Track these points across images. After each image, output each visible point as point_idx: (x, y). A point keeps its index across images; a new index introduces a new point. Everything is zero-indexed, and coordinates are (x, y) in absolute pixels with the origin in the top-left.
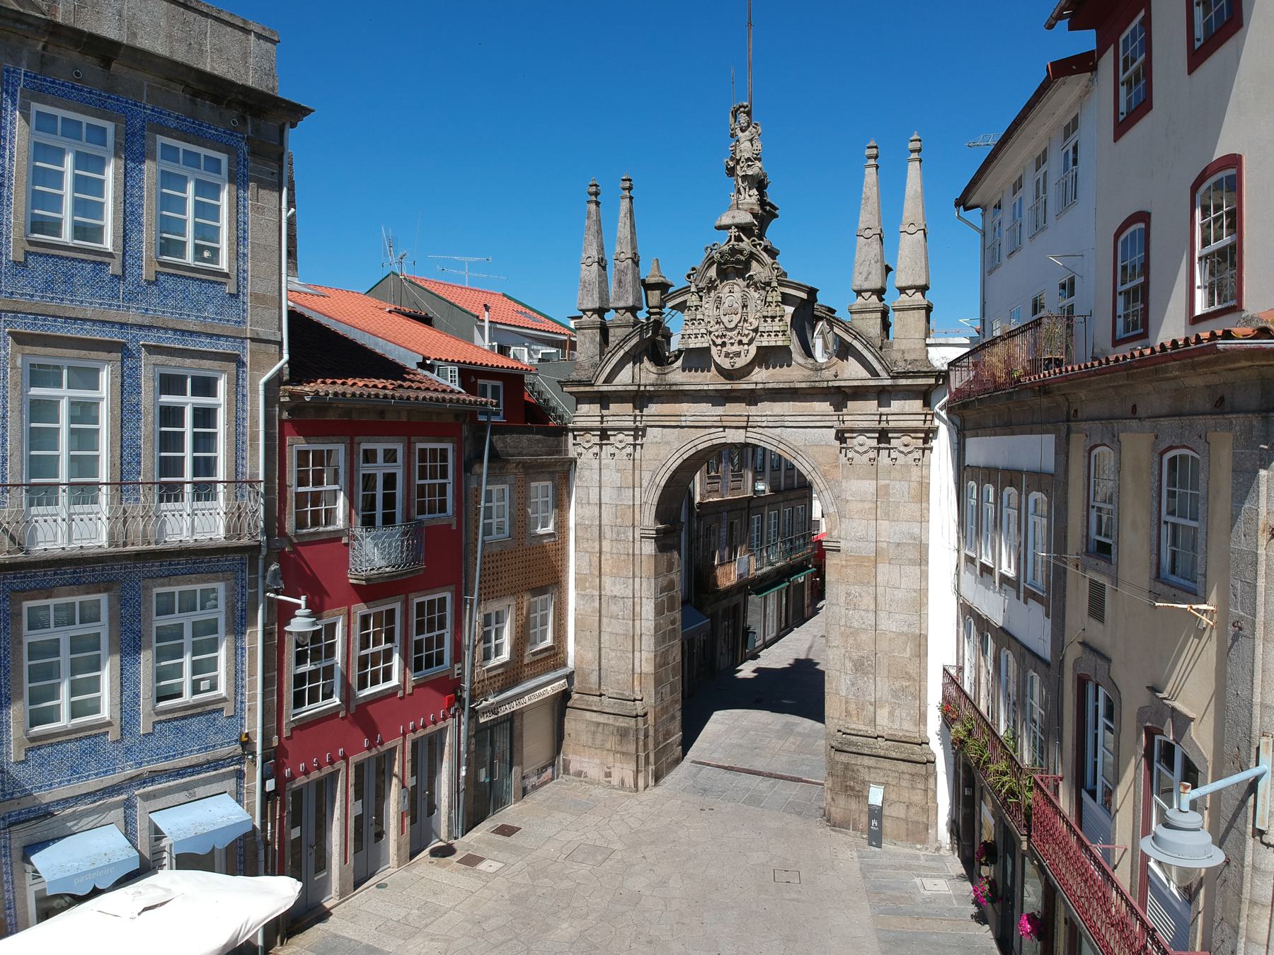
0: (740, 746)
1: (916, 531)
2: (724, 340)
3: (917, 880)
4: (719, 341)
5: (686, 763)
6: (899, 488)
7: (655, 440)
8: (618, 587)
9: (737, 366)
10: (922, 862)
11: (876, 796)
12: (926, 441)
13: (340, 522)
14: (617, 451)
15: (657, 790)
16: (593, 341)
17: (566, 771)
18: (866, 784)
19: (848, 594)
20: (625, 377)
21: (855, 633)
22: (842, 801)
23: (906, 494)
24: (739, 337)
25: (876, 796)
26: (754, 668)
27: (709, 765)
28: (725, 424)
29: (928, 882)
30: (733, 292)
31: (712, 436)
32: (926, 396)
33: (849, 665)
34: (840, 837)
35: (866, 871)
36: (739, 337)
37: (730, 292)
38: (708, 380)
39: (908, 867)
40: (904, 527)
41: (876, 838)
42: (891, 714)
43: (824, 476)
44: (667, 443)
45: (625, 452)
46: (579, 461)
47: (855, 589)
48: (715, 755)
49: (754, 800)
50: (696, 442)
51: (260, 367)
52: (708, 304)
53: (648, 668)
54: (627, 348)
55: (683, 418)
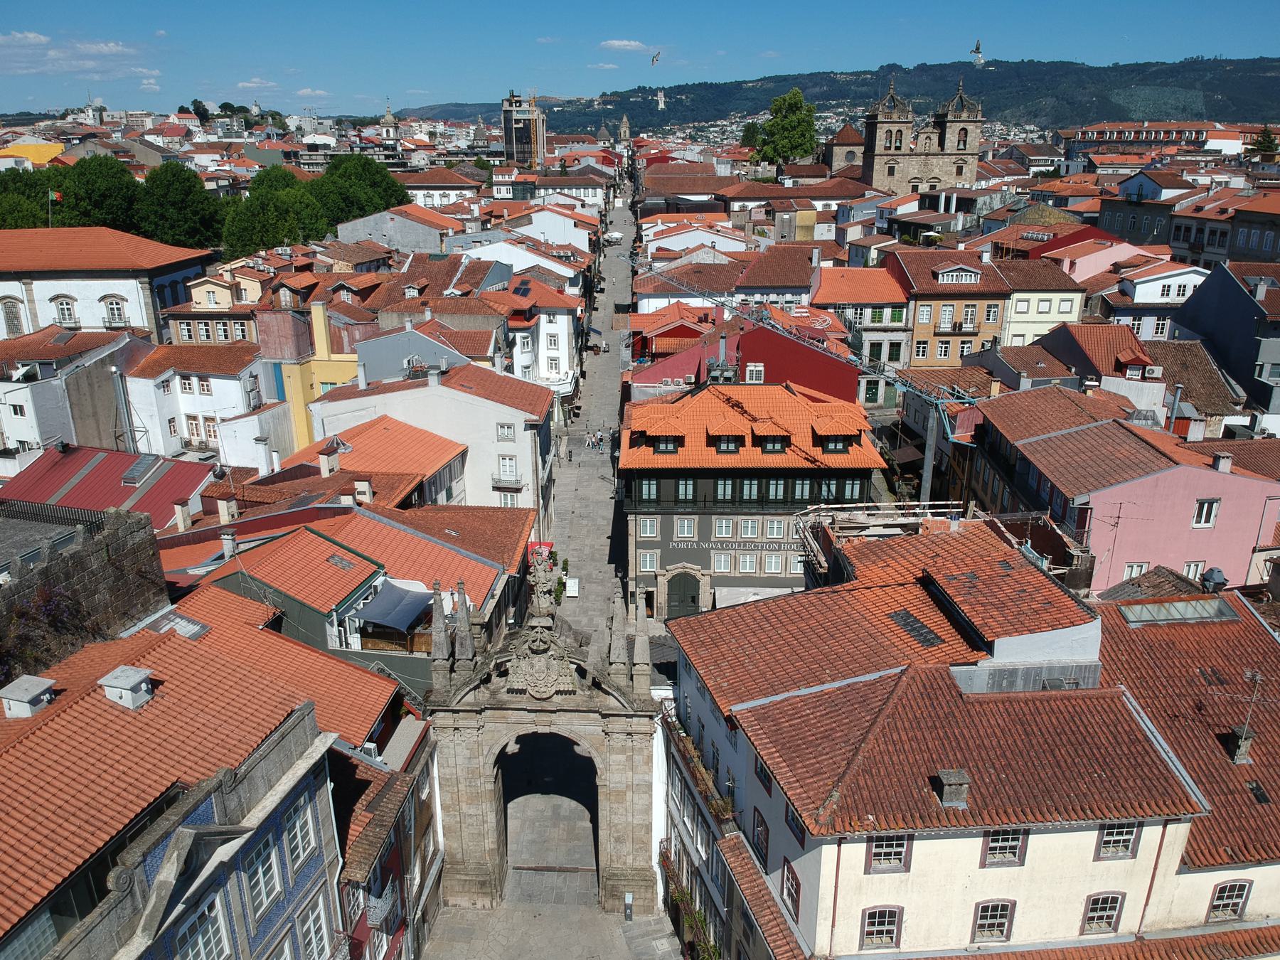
0: (533, 842)
3: (654, 943)
5: (510, 871)
6: (638, 758)
10: (654, 927)
11: (629, 899)
13: (362, 906)
15: (504, 905)
16: (444, 677)
17: (446, 904)
18: (623, 893)
19: (611, 808)
20: (470, 698)
21: (616, 825)
22: (611, 901)
25: (629, 899)
26: (514, 739)
27: (523, 869)
29: (658, 943)
30: (540, 661)
32: (651, 717)
33: (612, 840)
34: (613, 918)
35: (630, 941)
38: (523, 701)
39: (647, 934)
40: (641, 776)
41: (628, 917)
42: (634, 859)
46: (439, 744)
47: (615, 806)
48: (524, 856)
49: (559, 899)
51: (332, 876)
52: (523, 664)
53: (494, 846)
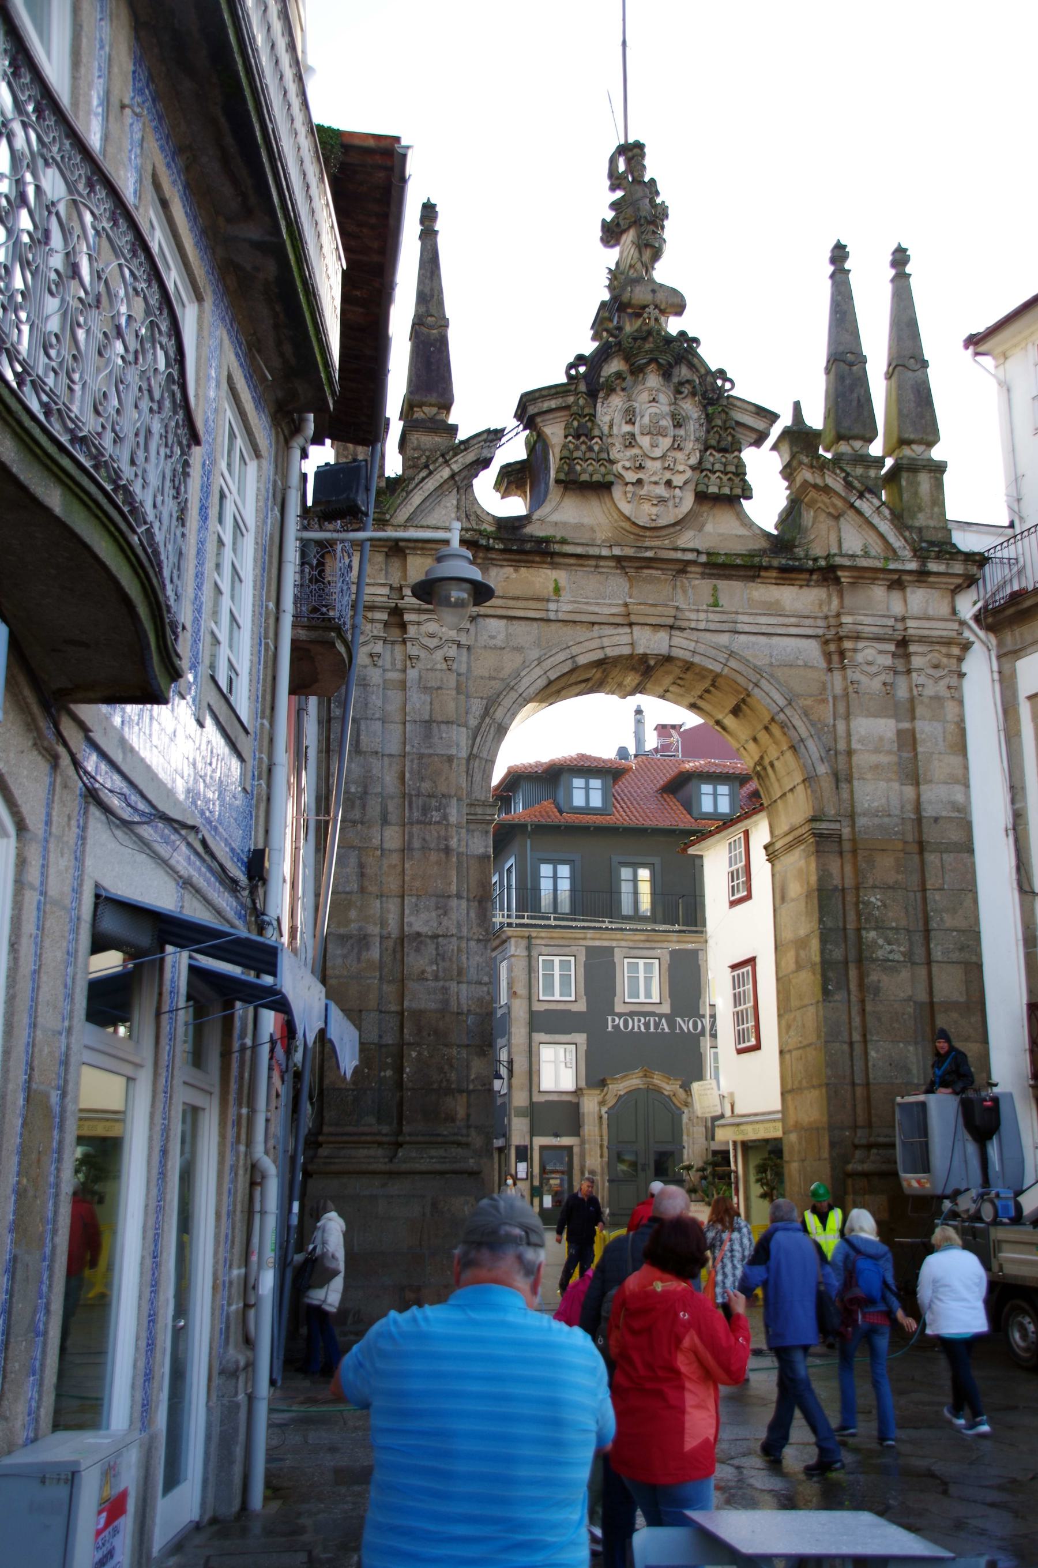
1: (959, 798)
2: (640, 475)
4: (631, 476)
7: (492, 643)
8: (424, 916)
9: (662, 522)
12: (960, 660)
14: (423, 654)
23: (941, 743)
24: (668, 475)
28: (633, 618)
31: (606, 642)
36: (668, 475)
37: (654, 400)
43: (806, 715)
44: (519, 649)
45: (439, 655)
50: (575, 650)
54: (456, 467)
55: (552, 606)
